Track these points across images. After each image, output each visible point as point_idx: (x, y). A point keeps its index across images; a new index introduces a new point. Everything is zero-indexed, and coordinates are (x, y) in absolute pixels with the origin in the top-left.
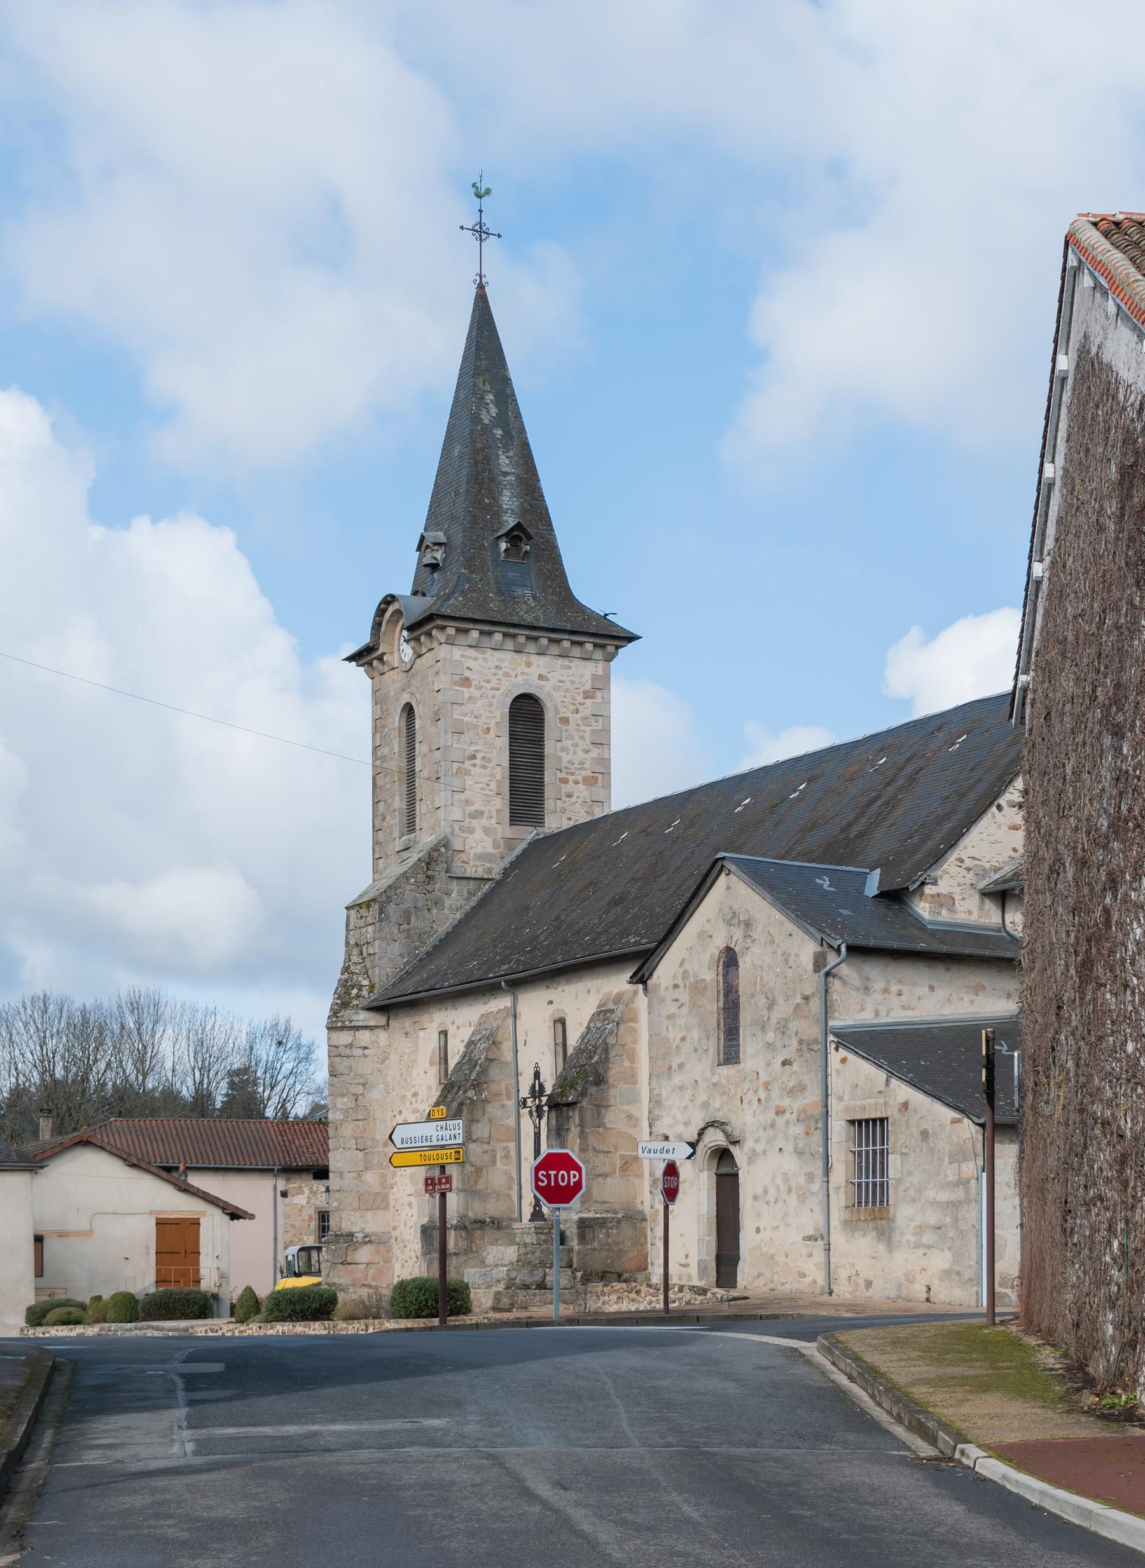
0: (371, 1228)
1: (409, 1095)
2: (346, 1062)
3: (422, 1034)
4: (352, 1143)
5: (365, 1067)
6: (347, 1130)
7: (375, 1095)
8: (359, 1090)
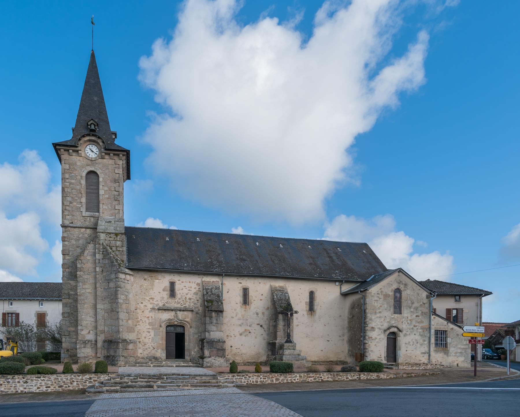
0: (130, 338)
1: (148, 298)
2: (123, 284)
3: (157, 281)
4: (125, 311)
5: (128, 287)
6: (124, 306)
7: (131, 296)
8: (127, 294)
